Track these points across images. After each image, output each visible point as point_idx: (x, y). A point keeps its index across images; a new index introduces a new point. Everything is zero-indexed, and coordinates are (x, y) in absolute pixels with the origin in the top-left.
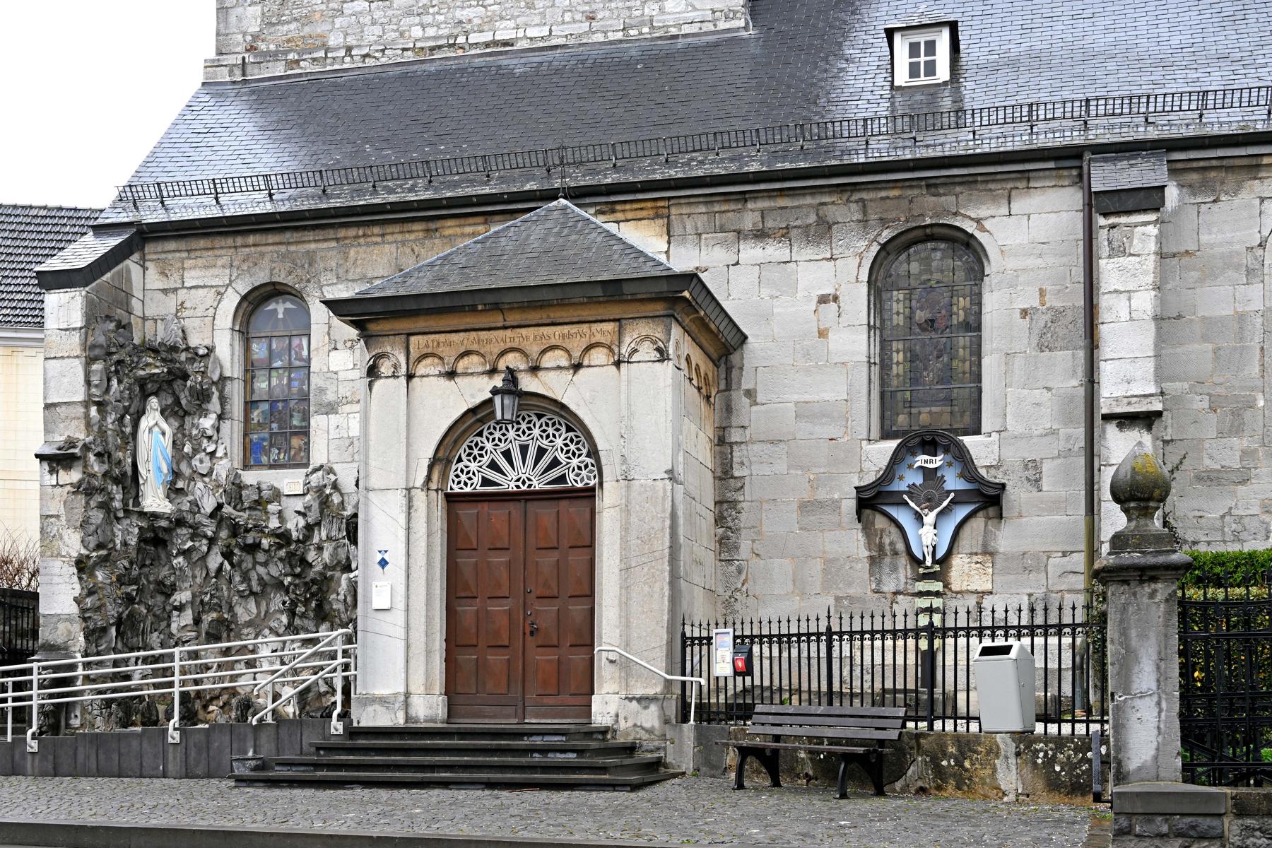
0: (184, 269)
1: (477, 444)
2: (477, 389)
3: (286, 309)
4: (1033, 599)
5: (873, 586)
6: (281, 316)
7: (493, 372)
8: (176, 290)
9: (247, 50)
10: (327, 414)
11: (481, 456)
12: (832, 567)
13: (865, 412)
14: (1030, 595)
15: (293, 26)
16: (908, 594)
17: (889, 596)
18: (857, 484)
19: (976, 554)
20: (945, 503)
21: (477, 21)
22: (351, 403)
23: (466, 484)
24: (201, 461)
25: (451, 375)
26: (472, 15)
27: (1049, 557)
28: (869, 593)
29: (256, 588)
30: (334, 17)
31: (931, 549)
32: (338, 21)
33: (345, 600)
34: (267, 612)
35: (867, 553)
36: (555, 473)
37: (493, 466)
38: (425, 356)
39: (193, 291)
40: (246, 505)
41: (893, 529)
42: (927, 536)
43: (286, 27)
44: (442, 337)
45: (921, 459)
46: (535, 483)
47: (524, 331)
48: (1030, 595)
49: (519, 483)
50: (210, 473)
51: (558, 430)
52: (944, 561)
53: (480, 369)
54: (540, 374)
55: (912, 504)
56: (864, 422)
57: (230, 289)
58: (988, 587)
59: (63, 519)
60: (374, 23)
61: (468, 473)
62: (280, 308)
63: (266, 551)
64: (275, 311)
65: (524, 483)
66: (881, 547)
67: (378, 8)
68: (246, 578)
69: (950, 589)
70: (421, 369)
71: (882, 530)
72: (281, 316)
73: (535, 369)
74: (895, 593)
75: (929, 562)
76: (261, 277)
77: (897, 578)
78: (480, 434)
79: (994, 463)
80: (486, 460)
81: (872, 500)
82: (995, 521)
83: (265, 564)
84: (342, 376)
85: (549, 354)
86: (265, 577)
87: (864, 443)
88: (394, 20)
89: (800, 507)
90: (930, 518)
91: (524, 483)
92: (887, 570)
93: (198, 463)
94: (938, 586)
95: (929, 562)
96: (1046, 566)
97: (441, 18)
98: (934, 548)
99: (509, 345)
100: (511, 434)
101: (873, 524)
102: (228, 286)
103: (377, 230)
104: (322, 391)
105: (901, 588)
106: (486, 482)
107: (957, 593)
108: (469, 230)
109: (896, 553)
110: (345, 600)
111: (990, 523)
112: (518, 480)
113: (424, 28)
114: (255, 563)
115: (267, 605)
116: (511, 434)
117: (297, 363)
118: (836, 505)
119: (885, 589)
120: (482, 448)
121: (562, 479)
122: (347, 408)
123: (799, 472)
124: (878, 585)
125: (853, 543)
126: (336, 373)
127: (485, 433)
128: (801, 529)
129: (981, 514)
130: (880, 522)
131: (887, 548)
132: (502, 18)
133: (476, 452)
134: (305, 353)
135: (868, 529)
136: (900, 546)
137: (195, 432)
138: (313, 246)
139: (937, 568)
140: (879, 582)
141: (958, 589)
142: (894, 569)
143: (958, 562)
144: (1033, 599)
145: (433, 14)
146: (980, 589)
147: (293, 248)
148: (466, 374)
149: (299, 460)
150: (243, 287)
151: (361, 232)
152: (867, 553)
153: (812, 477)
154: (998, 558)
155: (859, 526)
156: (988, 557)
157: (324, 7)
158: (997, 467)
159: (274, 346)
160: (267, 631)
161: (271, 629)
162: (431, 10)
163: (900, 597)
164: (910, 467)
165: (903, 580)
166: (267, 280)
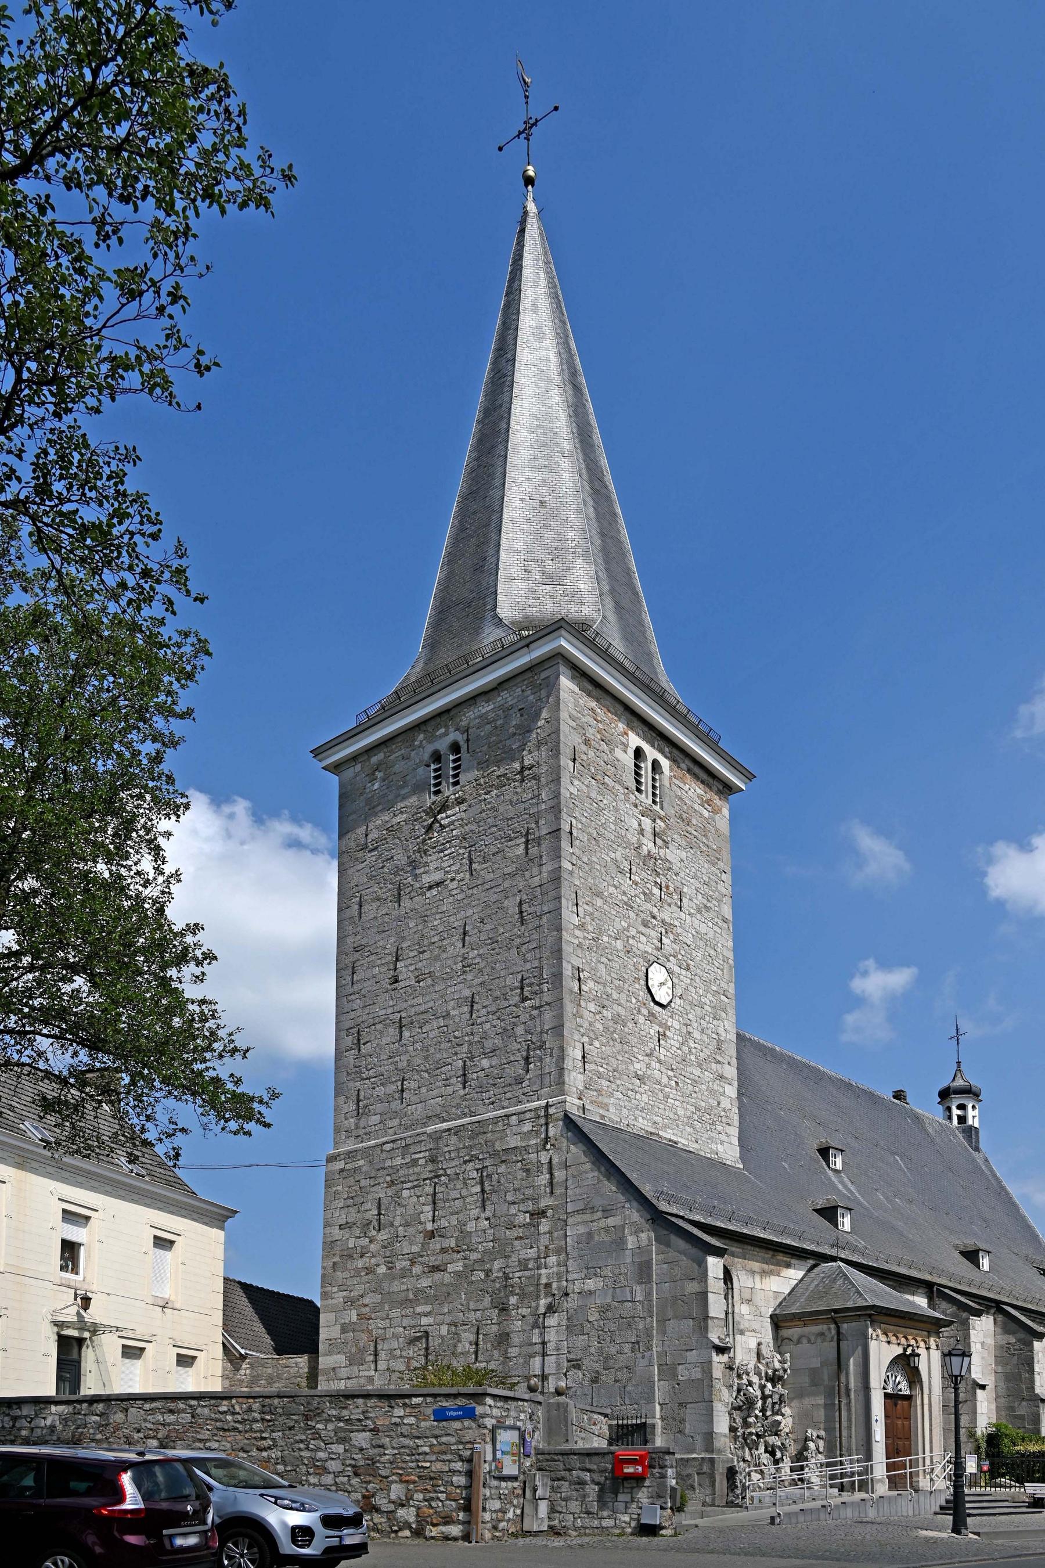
15: (595, 1093)
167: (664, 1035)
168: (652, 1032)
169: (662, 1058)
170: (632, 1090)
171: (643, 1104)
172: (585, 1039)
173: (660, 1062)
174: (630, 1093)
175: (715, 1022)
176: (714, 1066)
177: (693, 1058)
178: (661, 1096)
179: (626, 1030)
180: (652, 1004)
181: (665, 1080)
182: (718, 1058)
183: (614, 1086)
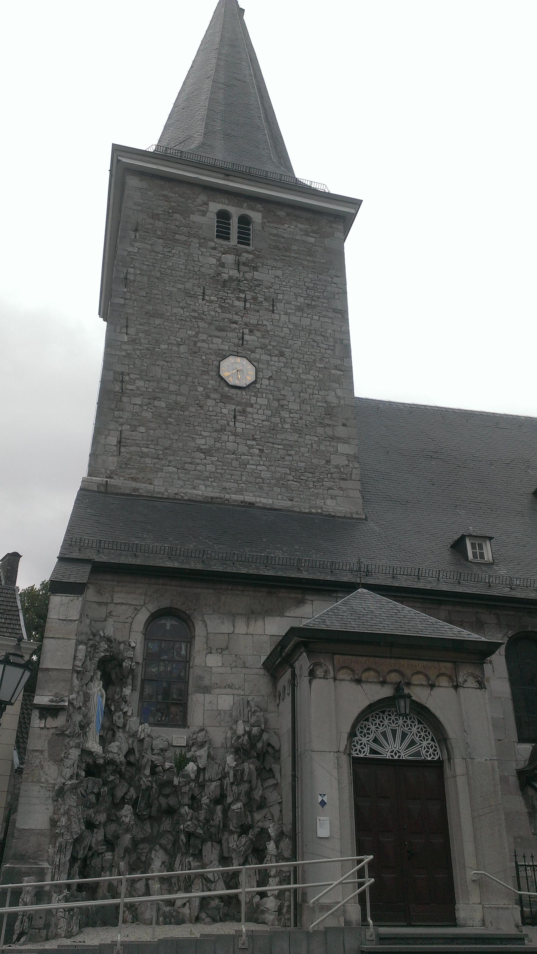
0: (114, 592)
1: (365, 726)
2: (387, 692)
3: (172, 625)
6: (168, 628)
7: (383, 683)
8: (106, 604)
9: (107, 478)
10: (204, 693)
11: (369, 734)
15: (134, 471)
21: (233, 489)
22: (220, 687)
23: (360, 752)
24: (119, 717)
25: (359, 681)
26: (231, 487)
29: (154, 813)
30: (157, 472)
32: (160, 474)
33: (219, 826)
34: (158, 831)
36: (413, 750)
37: (376, 740)
38: (343, 668)
39: (118, 606)
40: (156, 751)
43: (130, 471)
44: (353, 658)
46: (402, 754)
47: (401, 661)
49: (393, 754)
50: (125, 725)
51: (413, 722)
53: (376, 680)
54: (411, 687)
57: (144, 608)
59: (46, 754)
60: (179, 479)
61: (361, 744)
62: (169, 623)
63: (175, 786)
64: (165, 624)
65: (396, 754)
67: (182, 473)
68: (149, 806)
70: (340, 676)
72: (168, 628)
73: (409, 684)
76: (165, 603)
78: (367, 720)
80: (372, 737)
83: (167, 796)
84: (214, 670)
85: (415, 677)
86: (164, 806)
88: (190, 480)
91: (396, 754)
93: (117, 719)
97: (215, 484)
99: (393, 668)
100: (386, 722)
102: (142, 606)
103: (239, 588)
104: (201, 678)
106: (372, 751)
108: (293, 595)
110: (219, 826)
112: (392, 752)
113: (206, 487)
114: (160, 794)
115: (159, 826)
116: (401, 722)
117: (177, 658)
120: (369, 729)
121: (418, 754)
122: (217, 691)
126: (211, 668)
127: (370, 719)
132: (246, 491)
133: (365, 731)
134: (183, 652)
137: (117, 697)
138: (198, 591)
145: (211, 482)
147: (186, 590)
148: (367, 682)
149: (183, 724)
150: (153, 608)
151: (230, 587)
157: (152, 466)
159: (163, 646)
160: (157, 847)
161: (160, 845)
162: (210, 480)
166: (168, 605)
167: (244, 411)
168: (224, 411)
169: (239, 430)
170: (190, 463)
171: (207, 474)
172: (126, 427)
173: (235, 434)
174: (187, 466)
175: (322, 393)
176: (320, 430)
177: (287, 426)
178: (235, 463)
179: (187, 413)
180: (227, 389)
181: (243, 449)
182: (327, 422)
183: (163, 462)
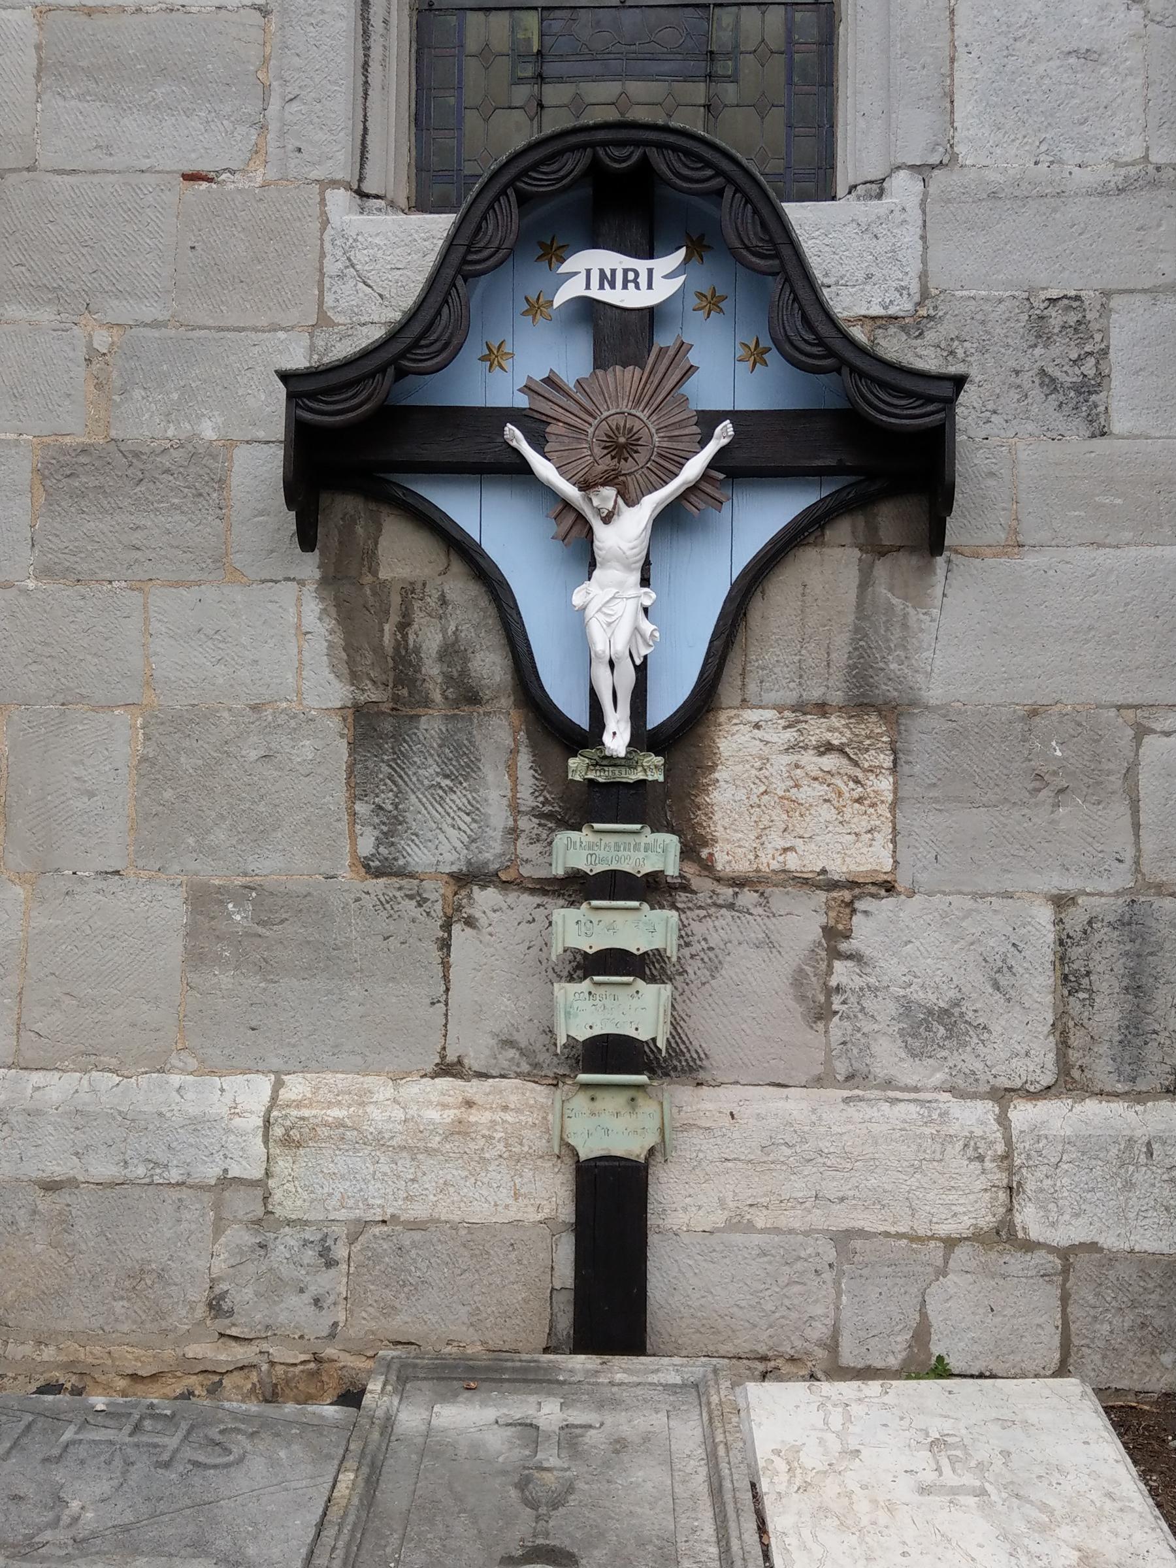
4: (1076, 919)
5: (366, 846)
12: (181, 759)
13: (344, 60)
14: (1061, 902)
16: (518, 884)
17: (436, 891)
18: (298, 360)
19: (822, 709)
20: (694, 468)
27: (1141, 732)
28: (346, 875)
31: (626, 678)
35: (338, 693)
41: (460, 589)
42: (617, 615)
45: (593, 272)
48: (1061, 902)
52: (681, 738)
55: (543, 468)
56: (340, 106)
58: (875, 858)
66: (402, 669)
69: (707, 867)
71: (410, 591)
74: (467, 879)
75: (617, 737)
77: (473, 811)
79: (902, 306)
81: (366, 446)
82: (907, 562)
87: (339, 199)
89: (41, 473)
90: (625, 531)
92: (430, 771)
94: (651, 851)
95: (617, 737)
96: (1131, 772)
98: (641, 670)
101: (370, 558)
105: (492, 852)
107: (739, 883)
109: (468, 696)
111: (881, 570)
118: (204, 470)
119: (419, 857)
123: (46, 316)
124: (386, 838)
125: (272, 640)
128: (45, 572)
129: (842, 530)
130: (402, 554)
131: (432, 669)
135: (347, 585)
136: (490, 666)
139: (651, 768)
140: (392, 825)
141: (743, 867)
142: (462, 766)
143: (745, 745)
144: (1076, 919)
146: (839, 869)
152: (338, 693)
153: (102, 340)
154: (922, 733)
155: (309, 566)
156: (874, 725)
158: (915, 325)
163: (485, 898)
164: (536, 307)
165: (498, 816)
